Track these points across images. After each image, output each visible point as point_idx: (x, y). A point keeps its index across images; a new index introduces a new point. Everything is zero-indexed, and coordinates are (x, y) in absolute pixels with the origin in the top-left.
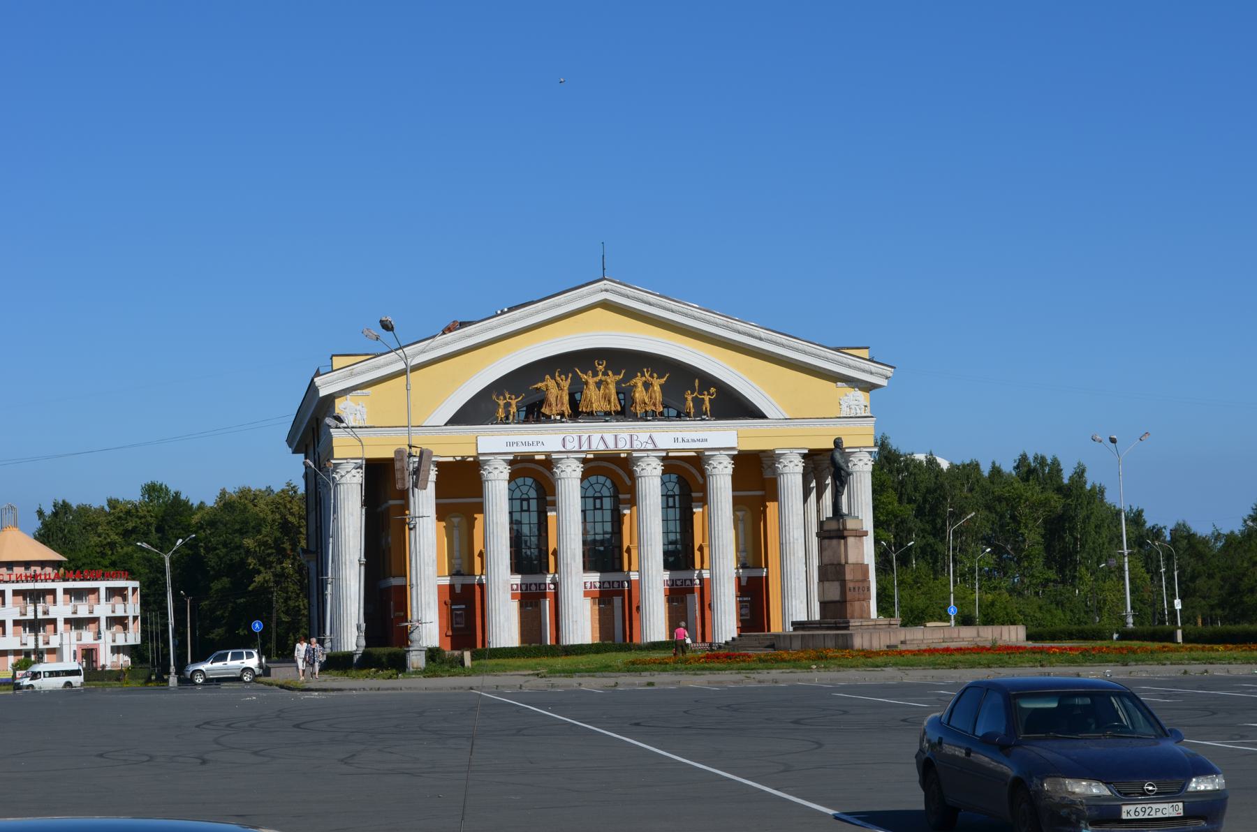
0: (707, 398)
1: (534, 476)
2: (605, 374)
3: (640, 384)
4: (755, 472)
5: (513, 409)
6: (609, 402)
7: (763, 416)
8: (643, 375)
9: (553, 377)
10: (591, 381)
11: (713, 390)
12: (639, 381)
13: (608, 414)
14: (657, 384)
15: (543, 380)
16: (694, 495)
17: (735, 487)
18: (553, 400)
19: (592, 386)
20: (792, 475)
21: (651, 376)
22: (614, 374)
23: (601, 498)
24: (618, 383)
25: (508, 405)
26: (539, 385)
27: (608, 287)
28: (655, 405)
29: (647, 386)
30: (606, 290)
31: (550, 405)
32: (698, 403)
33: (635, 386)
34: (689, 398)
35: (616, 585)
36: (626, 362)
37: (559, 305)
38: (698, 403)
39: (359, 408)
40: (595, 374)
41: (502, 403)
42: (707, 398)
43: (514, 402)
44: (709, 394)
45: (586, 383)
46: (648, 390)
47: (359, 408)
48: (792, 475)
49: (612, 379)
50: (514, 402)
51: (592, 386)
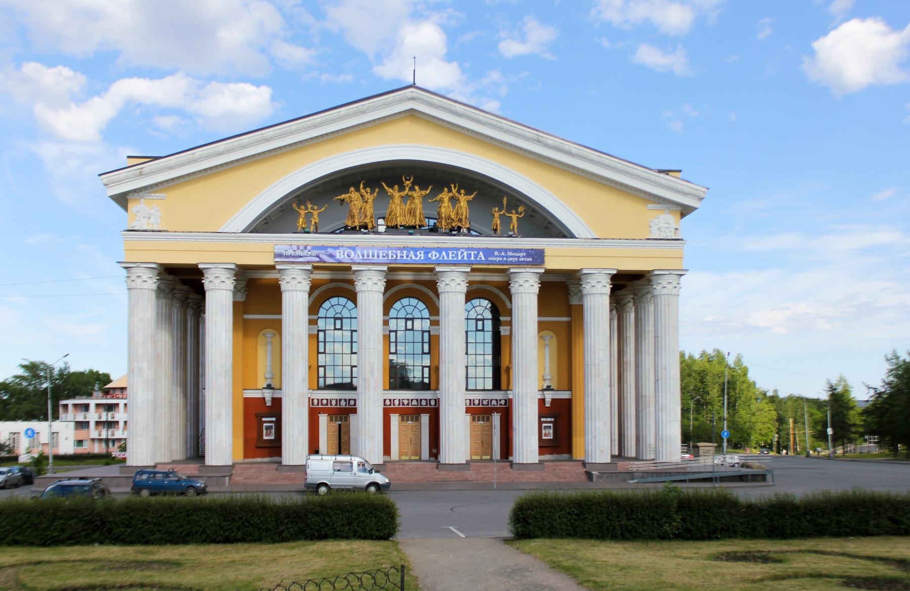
0: (514, 217)
1: (333, 286)
2: (412, 189)
3: (446, 199)
4: (561, 291)
5: (315, 219)
6: (415, 216)
7: (573, 236)
8: (450, 191)
9: (358, 190)
10: (397, 195)
11: (521, 209)
12: (445, 196)
13: (414, 227)
14: (464, 200)
15: (347, 192)
16: (502, 318)
17: (541, 312)
18: (355, 212)
19: (397, 200)
20: (597, 299)
21: (459, 192)
22: (421, 189)
23: (412, 319)
24: (425, 197)
25: (309, 215)
26: (343, 196)
27: (414, 95)
28: (460, 220)
29: (454, 200)
30: (413, 99)
31: (353, 217)
32: (506, 220)
33: (441, 201)
34: (497, 215)
35: (424, 403)
36: (433, 177)
37: (364, 112)
38: (506, 220)
39: (153, 211)
40: (402, 188)
41: (302, 212)
42: (514, 217)
43: (315, 213)
44: (517, 213)
45: (392, 197)
46: (454, 205)
47: (153, 211)
48: (597, 299)
49: (418, 193)
50: (315, 213)
51: (397, 200)
